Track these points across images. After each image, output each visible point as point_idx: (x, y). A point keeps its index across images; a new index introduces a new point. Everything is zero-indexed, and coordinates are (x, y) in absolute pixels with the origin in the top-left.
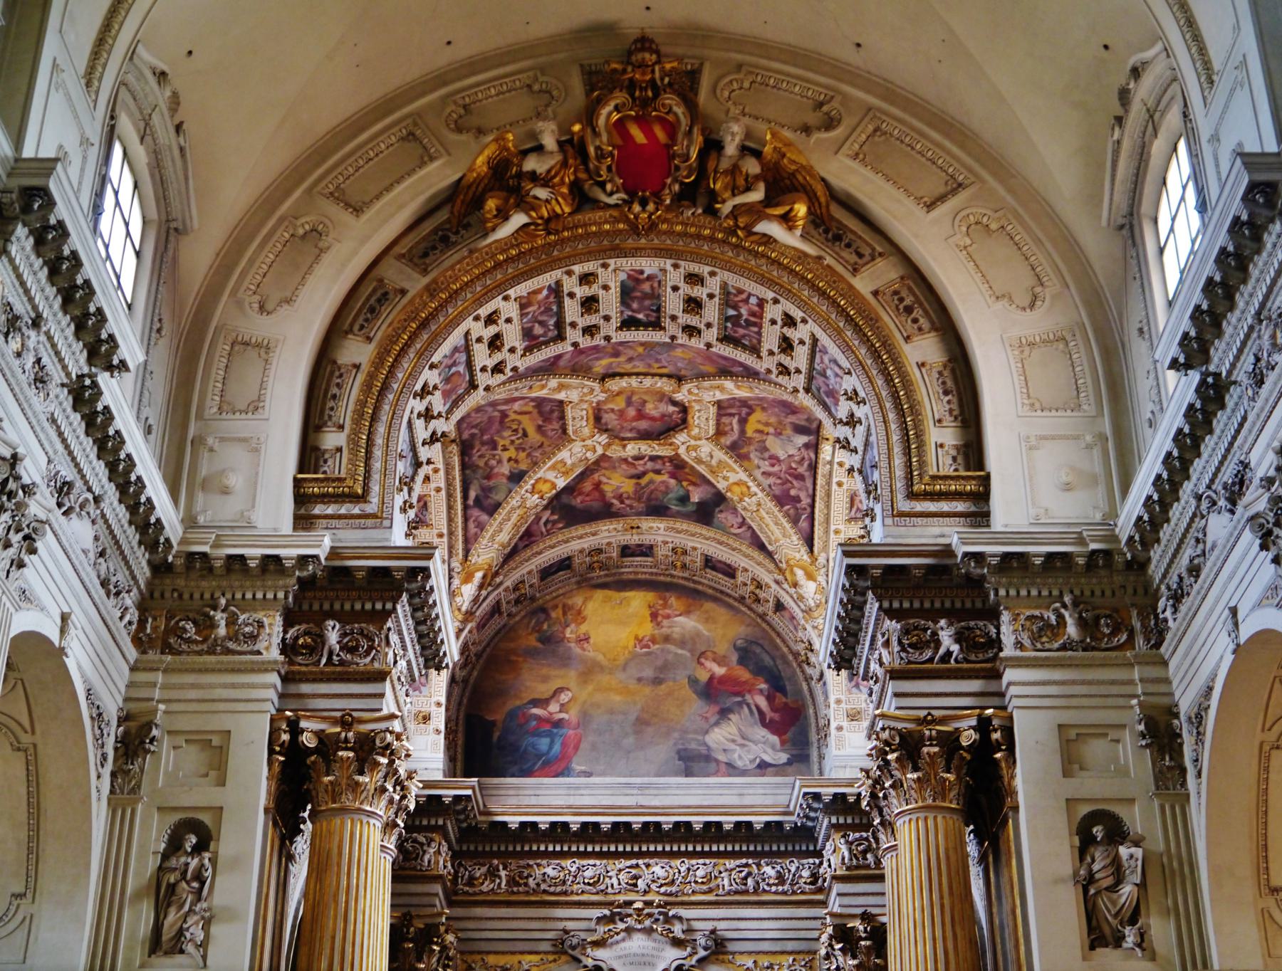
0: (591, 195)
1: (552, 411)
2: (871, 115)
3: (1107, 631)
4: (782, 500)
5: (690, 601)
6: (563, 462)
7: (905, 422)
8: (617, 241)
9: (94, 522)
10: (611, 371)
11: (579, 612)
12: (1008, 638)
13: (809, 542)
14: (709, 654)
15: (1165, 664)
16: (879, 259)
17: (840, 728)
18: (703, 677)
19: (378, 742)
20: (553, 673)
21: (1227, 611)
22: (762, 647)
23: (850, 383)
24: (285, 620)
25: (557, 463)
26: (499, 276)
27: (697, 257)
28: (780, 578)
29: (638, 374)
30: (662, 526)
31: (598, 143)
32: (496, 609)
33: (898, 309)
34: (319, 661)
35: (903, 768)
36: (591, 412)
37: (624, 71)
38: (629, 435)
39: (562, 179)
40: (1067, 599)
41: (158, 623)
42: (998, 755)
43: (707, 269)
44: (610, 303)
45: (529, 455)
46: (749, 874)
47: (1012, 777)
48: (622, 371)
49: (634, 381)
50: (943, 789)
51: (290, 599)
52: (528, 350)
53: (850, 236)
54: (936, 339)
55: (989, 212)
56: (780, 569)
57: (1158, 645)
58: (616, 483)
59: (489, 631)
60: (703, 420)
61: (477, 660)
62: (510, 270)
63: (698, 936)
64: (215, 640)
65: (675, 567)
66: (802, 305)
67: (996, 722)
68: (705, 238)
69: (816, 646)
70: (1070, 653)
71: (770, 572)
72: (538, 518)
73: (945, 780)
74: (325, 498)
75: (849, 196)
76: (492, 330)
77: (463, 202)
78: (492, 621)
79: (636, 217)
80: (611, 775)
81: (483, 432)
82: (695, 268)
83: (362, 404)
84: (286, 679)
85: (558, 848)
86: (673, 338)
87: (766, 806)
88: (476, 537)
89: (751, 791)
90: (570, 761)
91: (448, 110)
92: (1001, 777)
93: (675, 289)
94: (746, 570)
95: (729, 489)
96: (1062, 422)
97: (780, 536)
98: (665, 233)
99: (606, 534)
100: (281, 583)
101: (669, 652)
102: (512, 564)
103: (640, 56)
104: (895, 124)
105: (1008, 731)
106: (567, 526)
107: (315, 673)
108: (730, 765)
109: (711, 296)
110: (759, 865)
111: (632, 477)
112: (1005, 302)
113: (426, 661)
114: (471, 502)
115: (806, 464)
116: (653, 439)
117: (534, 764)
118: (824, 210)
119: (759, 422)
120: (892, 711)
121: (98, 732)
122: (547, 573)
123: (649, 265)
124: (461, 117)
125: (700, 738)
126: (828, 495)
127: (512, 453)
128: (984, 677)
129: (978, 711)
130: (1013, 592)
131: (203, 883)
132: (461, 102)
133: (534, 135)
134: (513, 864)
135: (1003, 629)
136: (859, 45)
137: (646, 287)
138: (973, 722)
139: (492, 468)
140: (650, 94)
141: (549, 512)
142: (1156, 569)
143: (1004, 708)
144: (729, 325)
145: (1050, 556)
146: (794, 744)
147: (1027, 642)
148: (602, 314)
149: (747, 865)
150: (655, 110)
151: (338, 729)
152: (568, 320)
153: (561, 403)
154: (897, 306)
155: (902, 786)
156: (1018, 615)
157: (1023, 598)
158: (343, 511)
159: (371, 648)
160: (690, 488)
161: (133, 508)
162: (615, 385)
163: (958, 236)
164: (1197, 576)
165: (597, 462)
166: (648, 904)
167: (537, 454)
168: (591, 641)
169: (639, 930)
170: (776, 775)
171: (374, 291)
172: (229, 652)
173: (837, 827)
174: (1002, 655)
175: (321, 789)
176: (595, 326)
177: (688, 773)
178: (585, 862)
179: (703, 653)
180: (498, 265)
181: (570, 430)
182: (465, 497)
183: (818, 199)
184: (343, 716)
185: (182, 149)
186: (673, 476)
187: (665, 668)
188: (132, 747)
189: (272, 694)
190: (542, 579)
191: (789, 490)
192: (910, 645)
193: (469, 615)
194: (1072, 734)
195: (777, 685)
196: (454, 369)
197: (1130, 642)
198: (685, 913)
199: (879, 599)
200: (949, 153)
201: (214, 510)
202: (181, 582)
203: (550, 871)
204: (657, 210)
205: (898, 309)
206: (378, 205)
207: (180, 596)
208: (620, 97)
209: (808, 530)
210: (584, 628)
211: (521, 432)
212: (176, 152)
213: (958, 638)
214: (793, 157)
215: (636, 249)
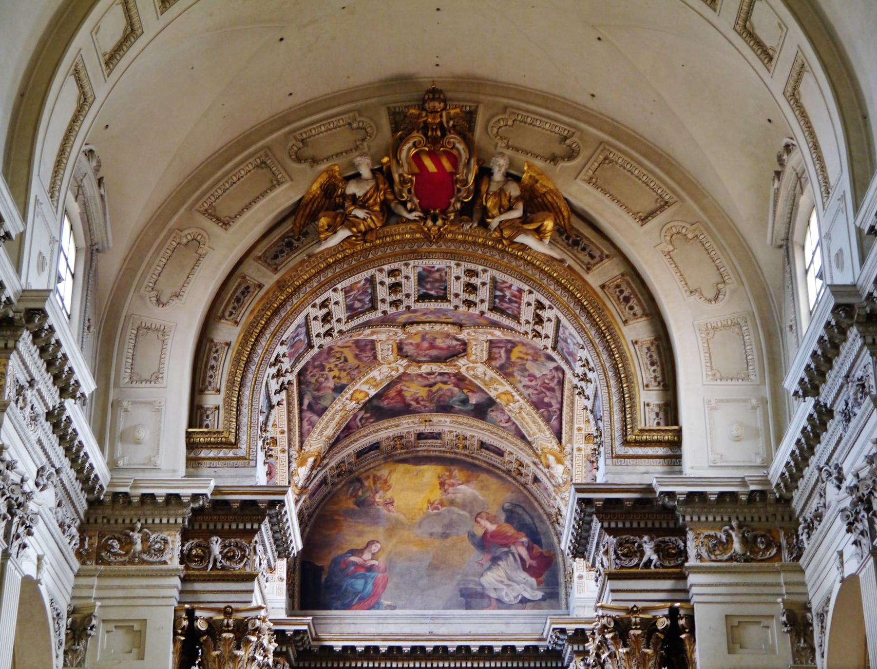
0: (396, 211)
1: (366, 345)
2: (601, 148)
3: (762, 547)
4: (538, 405)
5: (470, 472)
6: (374, 379)
7: (622, 387)
8: (415, 247)
9: (55, 487)
10: (410, 321)
11: (386, 482)
12: (692, 552)
13: (559, 435)
14: (484, 514)
15: (802, 571)
16: (606, 260)
17: (581, 577)
18: (479, 532)
19: (250, 626)
20: (366, 529)
21: (836, 554)
22: (524, 509)
23: (584, 354)
24: (182, 537)
25: (369, 379)
26: (330, 275)
27: (473, 258)
28: (537, 460)
29: (430, 322)
30: (448, 420)
31: (401, 172)
32: (324, 481)
33: (619, 299)
34: (207, 566)
35: (616, 644)
36: (395, 346)
38: (423, 359)
39: (375, 200)
40: (734, 524)
41: (92, 541)
42: (683, 636)
43: (480, 268)
44: (411, 286)
45: (349, 374)
47: (693, 652)
48: (419, 320)
49: (427, 327)
50: (644, 660)
51: (186, 523)
52: (350, 318)
53: (586, 242)
54: (646, 322)
55: (687, 225)
56: (537, 455)
57: (798, 558)
58: (413, 390)
59: (318, 498)
60: (479, 351)
61: (309, 520)
62: (338, 270)
64: (134, 553)
65: (458, 447)
66: (550, 296)
67: (682, 612)
68: (479, 244)
69: (564, 513)
70: (735, 563)
71: (530, 456)
72: (355, 416)
73: (646, 654)
74: (208, 445)
75: (585, 212)
76: (325, 311)
77: (302, 216)
79: (429, 230)
80: (410, 608)
83: (233, 374)
84: (184, 580)
86: (456, 307)
87: (526, 634)
88: (309, 431)
89: (515, 621)
90: (379, 598)
91: (290, 144)
92: (685, 651)
93: (458, 278)
94: (512, 454)
95: (498, 397)
96: (735, 388)
97: (537, 431)
98: (450, 240)
99: (407, 426)
100: (180, 511)
101: (454, 513)
102: (336, 450)
103: (432, 104)
104: (620, 155)
105: (691, 619)
106: (378, 420)
107: (205, 575)
108: (499, 601)
109: (484, 284)
111: (425, 386)
112: (696, 297)
113: (279, 553)
115: (556, 381)
116: (441, 362)
117: (352, 600)
118: (566, 221)
119: (521, 352)
120: (610, 604)
121: (57, 626)
122: (360, 454)
123: (438, 264)
124: (299, 149)
125: (476, 579)
127: (336, 372)
128: (674, 579)
129: (669, 604)
130: (695, 518)
132: (300, 137)
133: (353, 165)
135: (689, 543)
136: (593, 95)
137: (437, 275)
138: (666, 612)
139: (321, 383)
140: (439, 133)
142: (797, 503)
143: (688, 601)
144: (497, 300)
145: (722, 495)
146: (547, 585)
147: (705, 555)
148: (404, 293)
150: (443, 146)
151: (222, 617)
152: (379, 298)
153: (373, 341)
154: (618, 297)
155: (616, 656)
156: (699, 534)
157: (703, 522)
158: (221, 455)
159: (243, 556)
161: (79, 471)
162: (413, 329)
163: (664, 244)
164: (820, 521)
165: (400, 378)
167: (355, 373)
168: (395, 504)
170: (533, 608)
171: (239, 285)
172: (143, 562)
173: (578, 653)
174: (686, 564)
175: (211, 659)
176: (399, 300)
177: (468, 607)
179: (479, 514)
180: (329, 266)
181: (379, 357)
182: (301, 403)
183: (562, 213)
184: (226, 608)
185: (102, 196)
186: (456, 385)
187: (450, 525)
188: (78, 633)
189: (175, 593)
191: (543, 398)
192: (623, 555)
193: (304, 488)
194: (735, 622)
195: (535, 538)
196: (297, 339)
197: (778, 556)
199: (601, 521)
200: (659, 178)
201: (129, 456)
202: (108, 512)
204: (444, 224)
205: (619, 299)
206: (241, 220)
207: (109, 521)
208: (417, 136)
210: (389, 494)
212: (98, 199)
213: (657, 549)
214: (544, 183)
215: (429, 253)
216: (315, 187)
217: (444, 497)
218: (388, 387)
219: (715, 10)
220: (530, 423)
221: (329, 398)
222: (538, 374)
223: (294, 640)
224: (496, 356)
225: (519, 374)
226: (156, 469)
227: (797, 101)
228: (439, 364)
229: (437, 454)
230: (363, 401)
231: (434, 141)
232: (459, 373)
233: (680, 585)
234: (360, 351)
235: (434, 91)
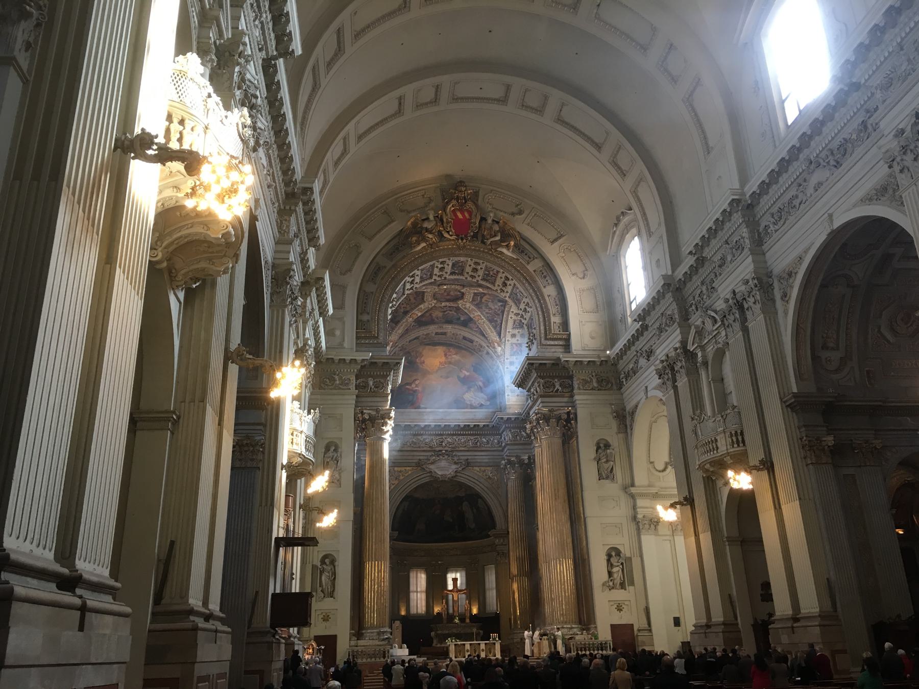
6: (421, 308)
12: (576, 386)
13: (499, 335)
18: (462, 376)
21: (644, 388)
28: (489, 345)
37: (455, 193)
44: (448, 269)
49: (449, 286)
52: (421, 282)
58: (437, 314)
60: (469, 296)
63: (461, 461)
65: (452, 339)
66: (512, 275)
74: (366, 338)
76: (412, 279)
82: (478, 261)
86: (466, 278)
93: (470, 266)
103: (460, 188)
105: (576, 414)
109: (481, 268)
112: (575, 276)
123: (462, 259)
126: (507, 321)
127: (405, 305)
131: (338, 462)
135: (574, 382)
137: (460, 264)
147: (581, 387)
158: (371, 342)
165: (432, 308)
166: (446, 451)
172: (340, 389)
208: (454, 202)
210: (422, 359)
216: (409, 223)
218: (427, 312)
219: (600, 153)
222: (493, 308)
226: (345, 348)
227: (636, 194)
231: (462, 205)
235: (461, 182)
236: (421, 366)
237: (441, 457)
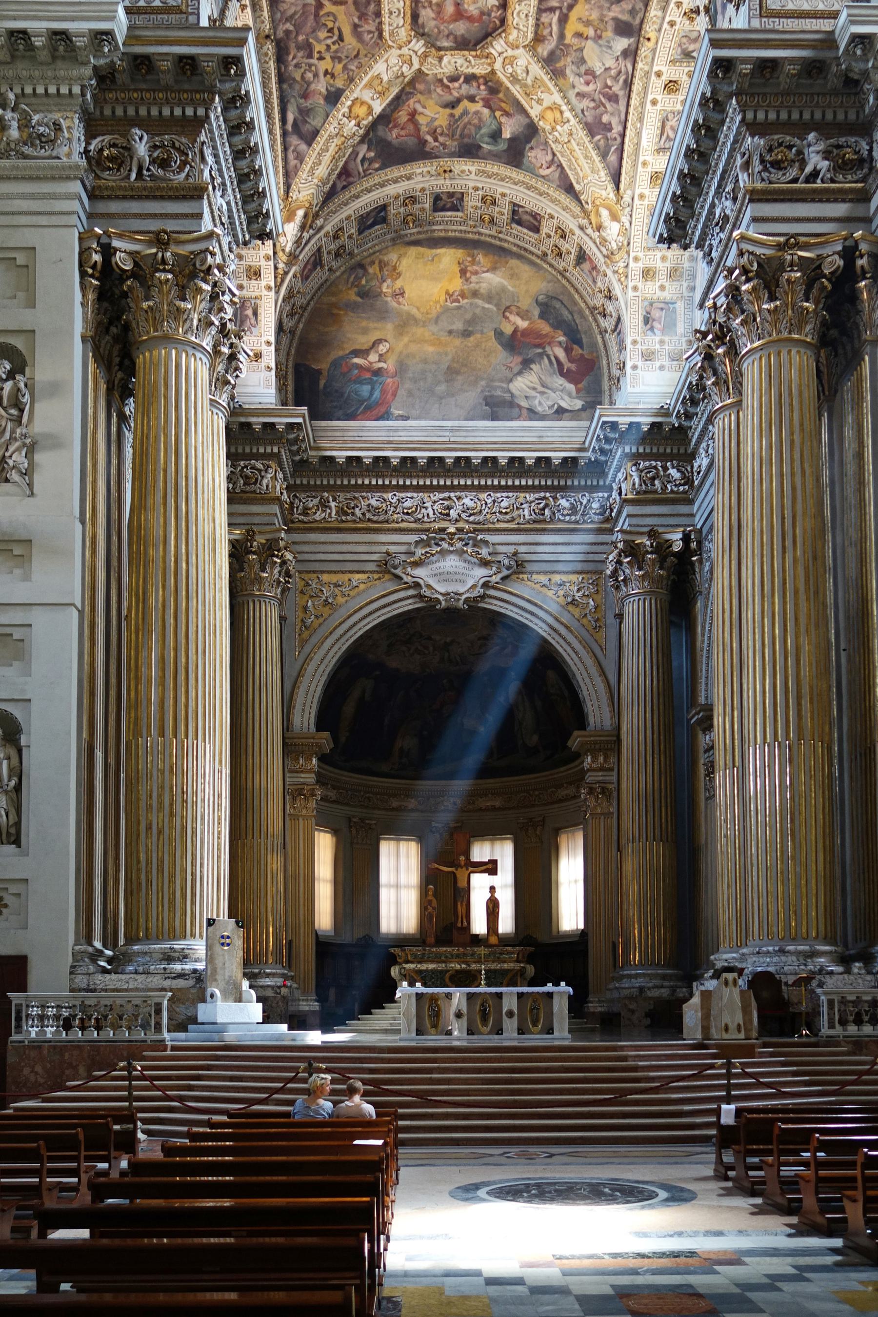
4: (594, 128)
5: (496, 258)
6: (378, 76)
11: (395, 268)
14: (513, 308)
17: (635, 367)
18: (508, 330)
20: (371, 325)
25: (373, 78)
28: (584, 222)
30: (473, 169)
38: (446, 44)
45: (345, 68)
46: (546, 505)
63: (500, 558)
72: (355, 154)
78: (314, 274)
80: (426, 419)
81: (298, 28)
85: (380, 482)
88: (296, 170)
94: (552, 217)
97: (589, 172)
100: (75, 72)
101: (477, 306)
102: (332, 206)
110: (555, 498)
114: (289, 127)
117: (357, 409)
125: (504, 385)
134: (342, 496)
141: (365, 147)
146: (588, 392)
149: (544, 498)
155: (755, 320)
160: (503, 120)
165: (412, 82)
168: (406, 295)
169: (451, 552)
177: (494, 417)
178: (403, 495)
179: (508, 308)
181: (386, 34)
182: (284, 120)
186: (487, 105)
190: (360, 232)
192: (771, 163)
193: (293, 257)
195: (574, 337)
198: (492, 538)
203: (373, 502)
209: (616, 164)
210: (399, 284)
211: (336, 31)
213: (827, 155)
217: (465, 287)
218: (397, 101)
220: (581, 157)
221: (321, 112)
223: (288, 440)
224: (546, 32)
225: (572, 71)
228: (466, 53)
229: (457, 234)
230: (365, 122)
232: (493, 72)
233: (859, 210)
234: (360, 18)
236: (394, 304)
237: (445, 545)
